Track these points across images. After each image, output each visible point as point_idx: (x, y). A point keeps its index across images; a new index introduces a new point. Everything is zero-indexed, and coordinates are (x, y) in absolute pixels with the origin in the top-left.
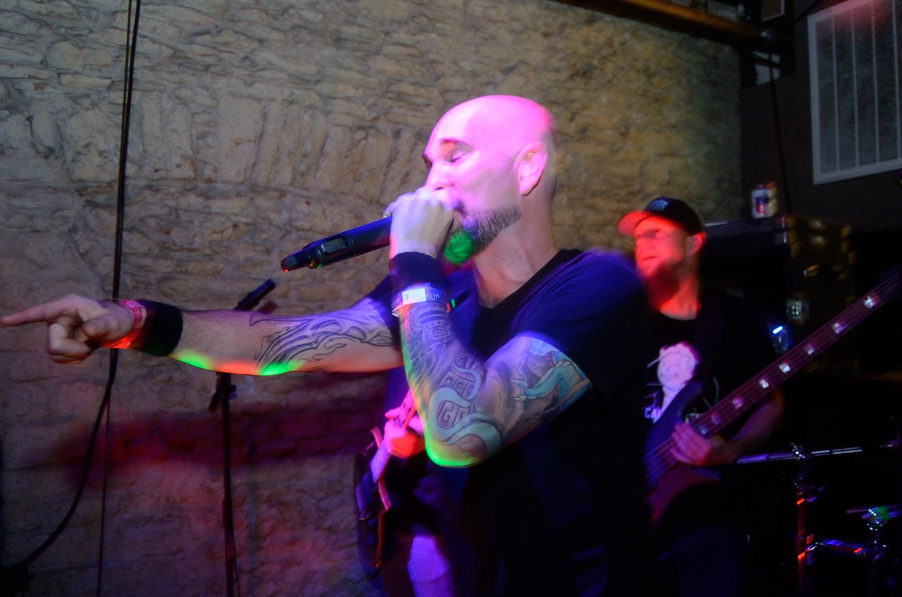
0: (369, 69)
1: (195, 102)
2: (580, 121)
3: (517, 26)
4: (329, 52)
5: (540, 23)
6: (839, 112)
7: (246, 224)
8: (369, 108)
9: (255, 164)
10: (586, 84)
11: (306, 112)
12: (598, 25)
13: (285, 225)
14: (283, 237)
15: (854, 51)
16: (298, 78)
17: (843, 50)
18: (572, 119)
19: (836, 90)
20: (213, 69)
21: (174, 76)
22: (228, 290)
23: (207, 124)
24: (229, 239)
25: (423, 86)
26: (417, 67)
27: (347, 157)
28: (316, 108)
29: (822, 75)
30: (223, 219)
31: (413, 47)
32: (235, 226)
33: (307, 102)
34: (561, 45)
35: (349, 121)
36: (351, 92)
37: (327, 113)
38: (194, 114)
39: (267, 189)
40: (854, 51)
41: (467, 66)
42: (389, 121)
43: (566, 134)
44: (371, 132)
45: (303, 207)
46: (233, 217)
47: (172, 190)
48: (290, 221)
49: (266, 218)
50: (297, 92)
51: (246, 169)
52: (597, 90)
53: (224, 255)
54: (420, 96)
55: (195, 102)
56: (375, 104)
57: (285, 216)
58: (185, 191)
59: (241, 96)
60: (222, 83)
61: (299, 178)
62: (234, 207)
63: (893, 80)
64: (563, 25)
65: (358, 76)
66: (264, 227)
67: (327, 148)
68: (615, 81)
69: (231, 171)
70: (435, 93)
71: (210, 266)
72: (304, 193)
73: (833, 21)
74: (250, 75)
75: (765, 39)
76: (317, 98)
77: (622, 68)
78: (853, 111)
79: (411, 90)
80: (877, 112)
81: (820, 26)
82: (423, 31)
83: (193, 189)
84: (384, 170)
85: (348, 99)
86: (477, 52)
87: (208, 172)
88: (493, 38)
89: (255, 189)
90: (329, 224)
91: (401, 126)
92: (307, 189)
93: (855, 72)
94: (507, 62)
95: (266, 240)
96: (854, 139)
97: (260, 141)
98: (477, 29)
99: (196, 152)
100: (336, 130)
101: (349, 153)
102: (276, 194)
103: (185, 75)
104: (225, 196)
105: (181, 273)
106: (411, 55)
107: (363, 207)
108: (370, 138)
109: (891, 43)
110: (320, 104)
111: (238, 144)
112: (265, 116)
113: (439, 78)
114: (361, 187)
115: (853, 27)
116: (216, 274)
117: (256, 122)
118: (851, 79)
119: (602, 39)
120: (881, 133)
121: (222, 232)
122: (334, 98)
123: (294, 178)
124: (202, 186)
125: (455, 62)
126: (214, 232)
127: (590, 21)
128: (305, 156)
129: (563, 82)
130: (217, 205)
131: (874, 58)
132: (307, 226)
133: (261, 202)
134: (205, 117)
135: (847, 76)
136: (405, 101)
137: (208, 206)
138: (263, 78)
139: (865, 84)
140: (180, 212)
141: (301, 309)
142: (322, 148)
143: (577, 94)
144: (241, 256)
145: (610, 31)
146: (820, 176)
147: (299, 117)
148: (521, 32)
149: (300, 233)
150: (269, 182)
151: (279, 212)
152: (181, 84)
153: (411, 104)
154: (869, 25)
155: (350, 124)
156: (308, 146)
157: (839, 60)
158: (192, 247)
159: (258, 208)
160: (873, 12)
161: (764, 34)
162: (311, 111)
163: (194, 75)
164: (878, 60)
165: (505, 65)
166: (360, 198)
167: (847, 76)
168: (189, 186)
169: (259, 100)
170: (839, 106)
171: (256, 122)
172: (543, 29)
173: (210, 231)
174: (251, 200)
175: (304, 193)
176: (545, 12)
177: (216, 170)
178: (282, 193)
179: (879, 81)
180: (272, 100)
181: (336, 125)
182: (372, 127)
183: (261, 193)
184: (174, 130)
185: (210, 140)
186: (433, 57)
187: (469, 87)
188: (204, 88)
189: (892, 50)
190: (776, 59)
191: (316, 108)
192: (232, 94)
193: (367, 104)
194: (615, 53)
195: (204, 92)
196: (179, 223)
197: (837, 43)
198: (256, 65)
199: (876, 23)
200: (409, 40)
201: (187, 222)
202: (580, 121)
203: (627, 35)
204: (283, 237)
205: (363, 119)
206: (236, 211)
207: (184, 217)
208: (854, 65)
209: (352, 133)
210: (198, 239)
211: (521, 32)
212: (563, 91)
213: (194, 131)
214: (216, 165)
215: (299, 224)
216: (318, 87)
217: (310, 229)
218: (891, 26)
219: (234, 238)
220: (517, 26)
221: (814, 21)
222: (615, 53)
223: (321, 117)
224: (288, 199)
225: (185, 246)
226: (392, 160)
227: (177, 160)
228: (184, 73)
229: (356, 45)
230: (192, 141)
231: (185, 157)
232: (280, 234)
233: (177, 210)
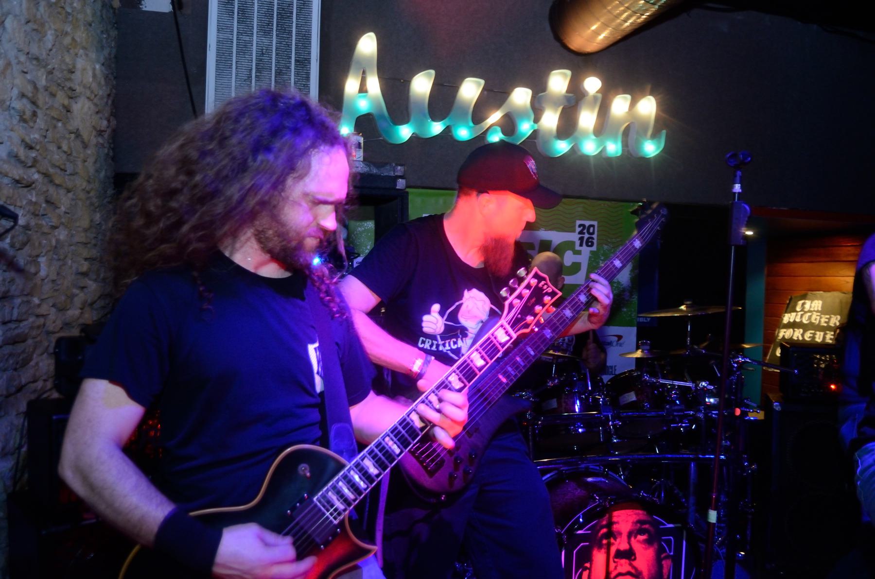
15: (255, 19)
40: (255, 19)
63: (290, 58)
78: (251, 70)
93: (255, 37)
109: (291, 27)
118: (251, 42)
135: (247, 38)
139: (263, 53)
154: (272, 4)
164: (277, 35)
167: (247, 38)
179: (277, 54)
189: (290, 32)
208: (255, 31)
218: (292, 13)
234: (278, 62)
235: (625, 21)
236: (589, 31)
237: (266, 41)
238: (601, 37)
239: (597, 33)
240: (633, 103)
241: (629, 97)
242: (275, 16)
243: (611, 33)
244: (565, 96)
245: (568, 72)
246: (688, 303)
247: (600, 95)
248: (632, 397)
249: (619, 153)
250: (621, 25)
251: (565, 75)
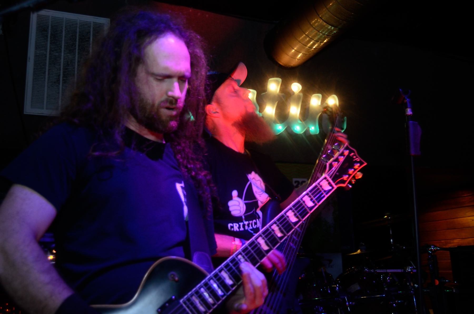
6: (49, 74)
15: (63, 42)
40: (63, 42)
78: (59, 75)
93: (63, 54)
96: (59, 93)
115: (64, 28)
135: (57, 54)
146: (29, 109)
160: (78, 26)
164: (79, 53)
167: (57, 54)
170: (49, 70)
199: (80, 32)
208: (63, 49)
218: (89, 38)
235: (317, 41)
236: (293, 50)
238: (300, 55)
239: (298, 52)
240: (324, 100)
241: (320, 95)
242: (77, 40)
243: (308, 51)
244: (279, 95)
245: (280, 80)
246: (388, 214)
247: (301, 94)
248: (356, 287)
249: (318, 132)
250: (313, 44)
251: (277, 81)
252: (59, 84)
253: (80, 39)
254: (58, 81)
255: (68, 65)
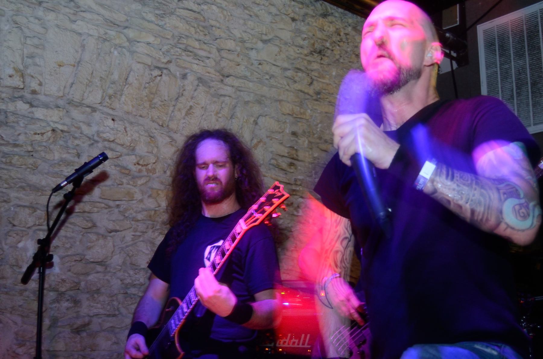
0: (165, 24)
1: (28, 28)
2: (317, 86)
3: (273, 10)
4: (136, 6)
5: (290, 11)
6: (502, 92)
7: (62, 131)
8: (164, 54)
9: (72, 84)
10: (322, 59)
11: (115, 48)
12: (330, 18)
13: (93, 135)
14: (92, 144)
15: (511, 49)
16: (111, 22)
17: (503, 49)
18: (311, 84)
19: (499, 76)
20: (45, 5)
21: (13, 5)
22: (44, 183)
23: (36, 47)
24: (46, 141)
25: (205, 43)
26: (201, 28)
27: (145, 88)
28: (124, 47)
29: (488, 67)
30: (44, 124)
31: (198, 13)
32: (53, 130)
33: (117, 42)
34: (304, 29)
35: (149, 61)
36: (151, 39)
37: (132, 53)
38: (26, 37)
39: (80, 105)
40: (511, 49)
41: (237, 33)
42: (178, 66)
43: (308, 94)
44: (165, 71)
45: (110, 123)
46: (52, 124)
47: (3, 95)
48: (98, 133)
49: (79, 128)
50: (109, 32)
51: (65, 87)
52: (329, 65)
53: (43, 154)
54: (202, 49)
55: (28, 28)
56: (168, 51)
57: (94, 129)
58: (13, 99)
59: (66, 29)
60: (51, 16)
61: (107, 98)
62: (53, 117)
64: (306, 15)
65: (158, 28)
66: (77, 135)
67: (131, 79)
68: (341, 61)
69: (52, 88)
70: (214, 51)
71: (31, 161)
72: (111, 112)
73: (496, 29)
74: (74, 14)
75: (449, 38)
76: (126, 40)
77: (346, 52)
78: (512, 90)
79: (196, 44)
80: (530, 91)
81: (485, 32)
82: (206, 3)
83: (21, 98)
84: (173, 103)
85: (148, 44)
86: (245, 24)
87: (34, 85)
88: (257, 16)
89: (70, 102)
90: (129, 138)
91: (187, 71)
92: (113, 109)
93: (513, 63)
94: (266, 35)
95: (78, 145)
97: (78, 66)
98: (245, 8)
99: (26, 67)
100: (139, 66)
101: (147, 85)
102: (88, 109)
103: (22, 6)
104: (46, 106)
105: (6, 163)
106: (196, 19)
107: (156, 129)
108: (163, 75)
110: (127, 44)
111: (60, 66)
112: (83, 47)
113: (217, 39)
114: (155, 114)
115: (510, 32)
116: (35, 168)
117: (77, 52)
118: (510, 68)
119: (332, 29)
120: (534, 106)
121: (42, 134)
122: (138, 42)
123: (103, 98)
124: (28, 96)
125: (228, 29)
126: (35, 134)
127: (325, 15)
128: (114, 83)
129: (306, 55)
130: (39, 113)
131: (527, 54)
132: (112, 139)
133: (75, 113)
134: (36, 41)
135: (507, 66)
136: (191, 52)
137: (33, 113)
138: (84, 18)
139: (520, 72)
140: (9, 114)
141: (103, 205)
142: (126, 79)
143: (315, 66)
144: (57, 156)
145: (339, 25)
147: (111, 52)
148: (277, 15)
149: (106, 143)
150: (83, 99)
151: (89, 125)
152: (18, 12)
153: (196, 55)
154: (522, 31)
155: (150, 64)
156: (116, 76)
157: (500, 56)
158: (17, 143)
159: (73, 119)
161: (448, 35)
162: (120, 49)
163: (28, 6)
164: (529, 55)
165: (265, 38)
166: (153, 121)
167: (507, 66)
168: (17, 94)
169: (80, 34)
171: (77, 52)
172: (292, 15)
173: (32, 133)
174: (67, 112)
175: (111, 112)
176: (293, 3)
177: (40, 84)
178: (94, 110)
179: (531, 69)
180: (91, 35)
181: (139, 62)
182: (166, 69)
183: (77, 106)
184: (9, 47)
185: (37, 60)
186: (213, 23)
187: (238, 49)
188: (36, 18)
190: (454, 54)
191: (124, 47)
192: (58, 26)
193: (163, 50)
194: (341, 41)
195: (37, 21)
196: (7, 123)
197: (499, 44)
198: (78, 7)
199: (527, 29)
200: (195, 7)
201: (13, 122)
202: (317, 86)
203: (350, 29)
204: (92, 144)
205: (159, 61)
206: (55, 119)
207: (11, 118)
208: (512, 58)
209: (151, 70)
210: (22, 138)
211: (277, 15)
212: (305, 62)
213: (25, 50)
214: (41, 80)
215: (104, 135)
216: (126, 31)
217: (113, 141)
219: (51, 140)
220: (273, 10)
221: (481, 29)
222: (341, 41)
223: (127, 54)
224: (97, 116)
225: (11, 142)
226: (180, 95)
227: (10, 71)
228: (22, 4)
229: (157, 4)
230: (23, 60)
231: (16, 70)
232: (89, 143)
233: (6, 112)
234: (532, 75)
237: (521, 62)
242: (526, 40)
252: (513, 99)
253: (529, 37)
254: (512, 96)
255: (520, 73)
